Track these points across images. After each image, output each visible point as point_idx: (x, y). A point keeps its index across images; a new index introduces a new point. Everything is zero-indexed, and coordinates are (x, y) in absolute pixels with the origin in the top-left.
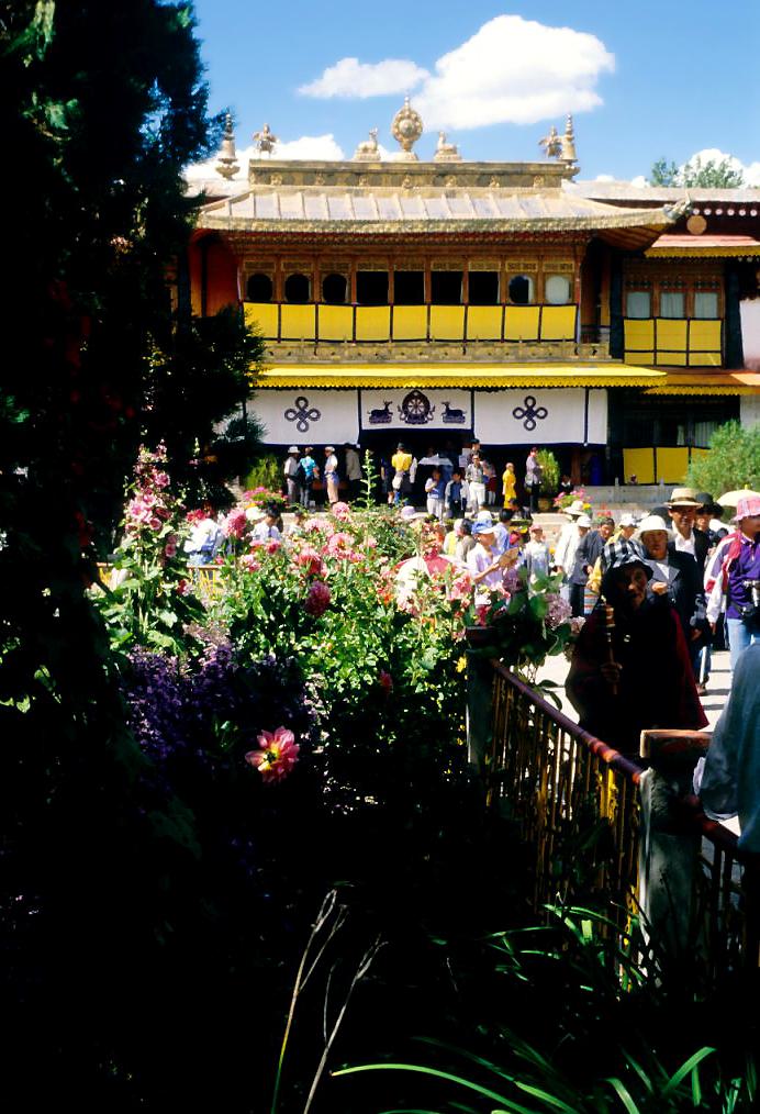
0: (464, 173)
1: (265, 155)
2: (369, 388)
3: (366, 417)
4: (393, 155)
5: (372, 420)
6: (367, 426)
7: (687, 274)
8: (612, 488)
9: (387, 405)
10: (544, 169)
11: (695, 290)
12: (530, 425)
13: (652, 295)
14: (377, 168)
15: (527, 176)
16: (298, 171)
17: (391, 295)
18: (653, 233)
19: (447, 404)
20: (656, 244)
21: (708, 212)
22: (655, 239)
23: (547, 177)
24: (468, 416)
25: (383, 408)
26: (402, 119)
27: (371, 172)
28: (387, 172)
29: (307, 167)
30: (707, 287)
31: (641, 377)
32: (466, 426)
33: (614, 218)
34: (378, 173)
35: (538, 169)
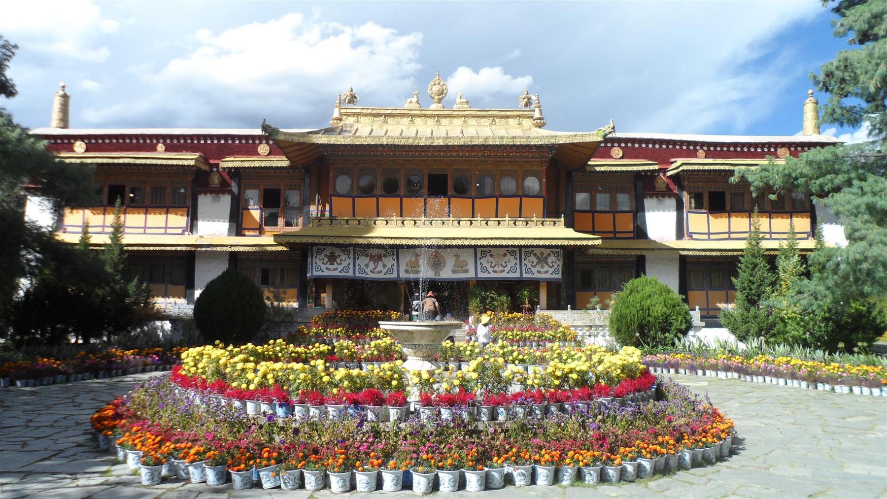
11: (617, 192)
21: (623, 145)
30: (623, 191)
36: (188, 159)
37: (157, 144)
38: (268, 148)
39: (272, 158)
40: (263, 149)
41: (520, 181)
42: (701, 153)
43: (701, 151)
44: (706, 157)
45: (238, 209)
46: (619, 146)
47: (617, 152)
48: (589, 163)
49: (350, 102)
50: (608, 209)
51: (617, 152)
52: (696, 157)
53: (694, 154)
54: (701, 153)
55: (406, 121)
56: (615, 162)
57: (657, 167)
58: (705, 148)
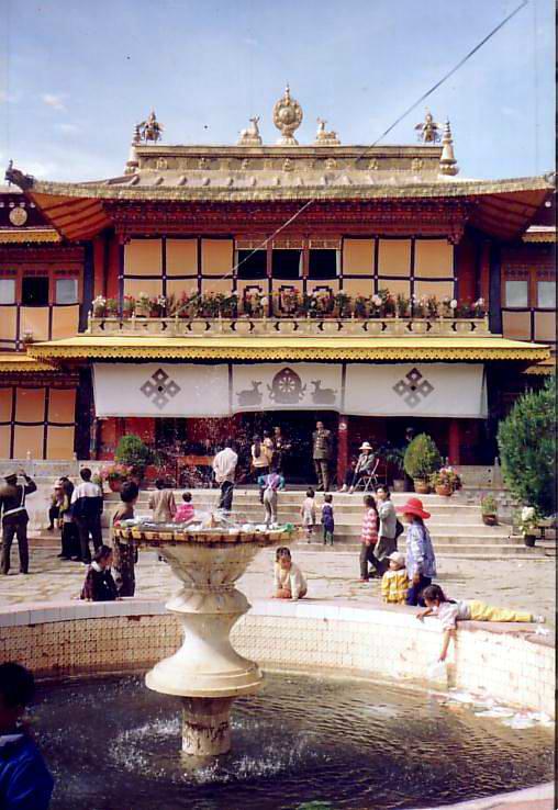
0: (343, 157)
8: (491, 468)
9: (256, 385)
10: (421, 151)
13: (529, 285)
14: (259, 152)
15: (405, 160)
16: (181, 156)
17: (269, 272)
19: (317, 384)
20: (528, 231)
23: (425, 160)
24: (338, 395)
26: (282, 106)
27: (250, 157)
28: (268, 156)
29: (190, 151)
34: (259, 157)
35: (415, 151)
38: (25, 214)
39: (32, 230)
40: (18, 215)
48: (528, 231)
49: (150, 137)
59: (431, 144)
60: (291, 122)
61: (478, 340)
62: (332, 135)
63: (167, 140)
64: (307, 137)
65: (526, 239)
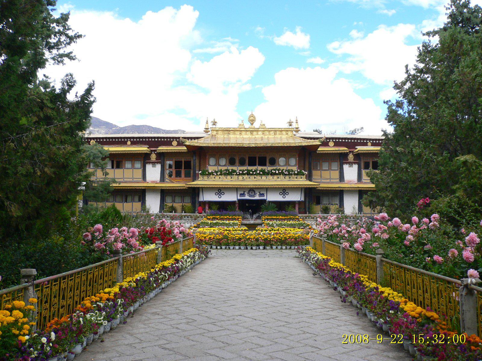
1: (214, 126)
2: (240, 188)
3: (239, 195)
4: (247, 125)
5: (240, 196)
6: (239, 198)
7: (330, 157)
9: (244, 192)
12: (284, 197)
18: (318, 146)
19: (260, 192)
20: (319, 149)
21: (334, 140)
22: (318, 148)
24: (265, 195)
25: (243, 193)
31: (313, 185)
32: (265, 198)
33: (305, 143)
36: (144, 149)
37: (127, 141)
40: (175, 143)
41: (287, 160)
42: (369, 144)
43: (369, 143)
44: (372, 146)
45: (164, 170)
46: (333, 141)
47: (331, 144)
50: (327, 169)
51: (331, 144)
52: (367, 145)
53: (366, 144)
54: (369, 144)
55: (238, 133)
56: (331, 148)
57: (348, 151)
58: (371, 142)
59: (290, 127)
60: (252, 121)
61: (302, 182)
62: (264, 125)
63: (218, 126)
64: (256, 125)
65: (318, 152)
